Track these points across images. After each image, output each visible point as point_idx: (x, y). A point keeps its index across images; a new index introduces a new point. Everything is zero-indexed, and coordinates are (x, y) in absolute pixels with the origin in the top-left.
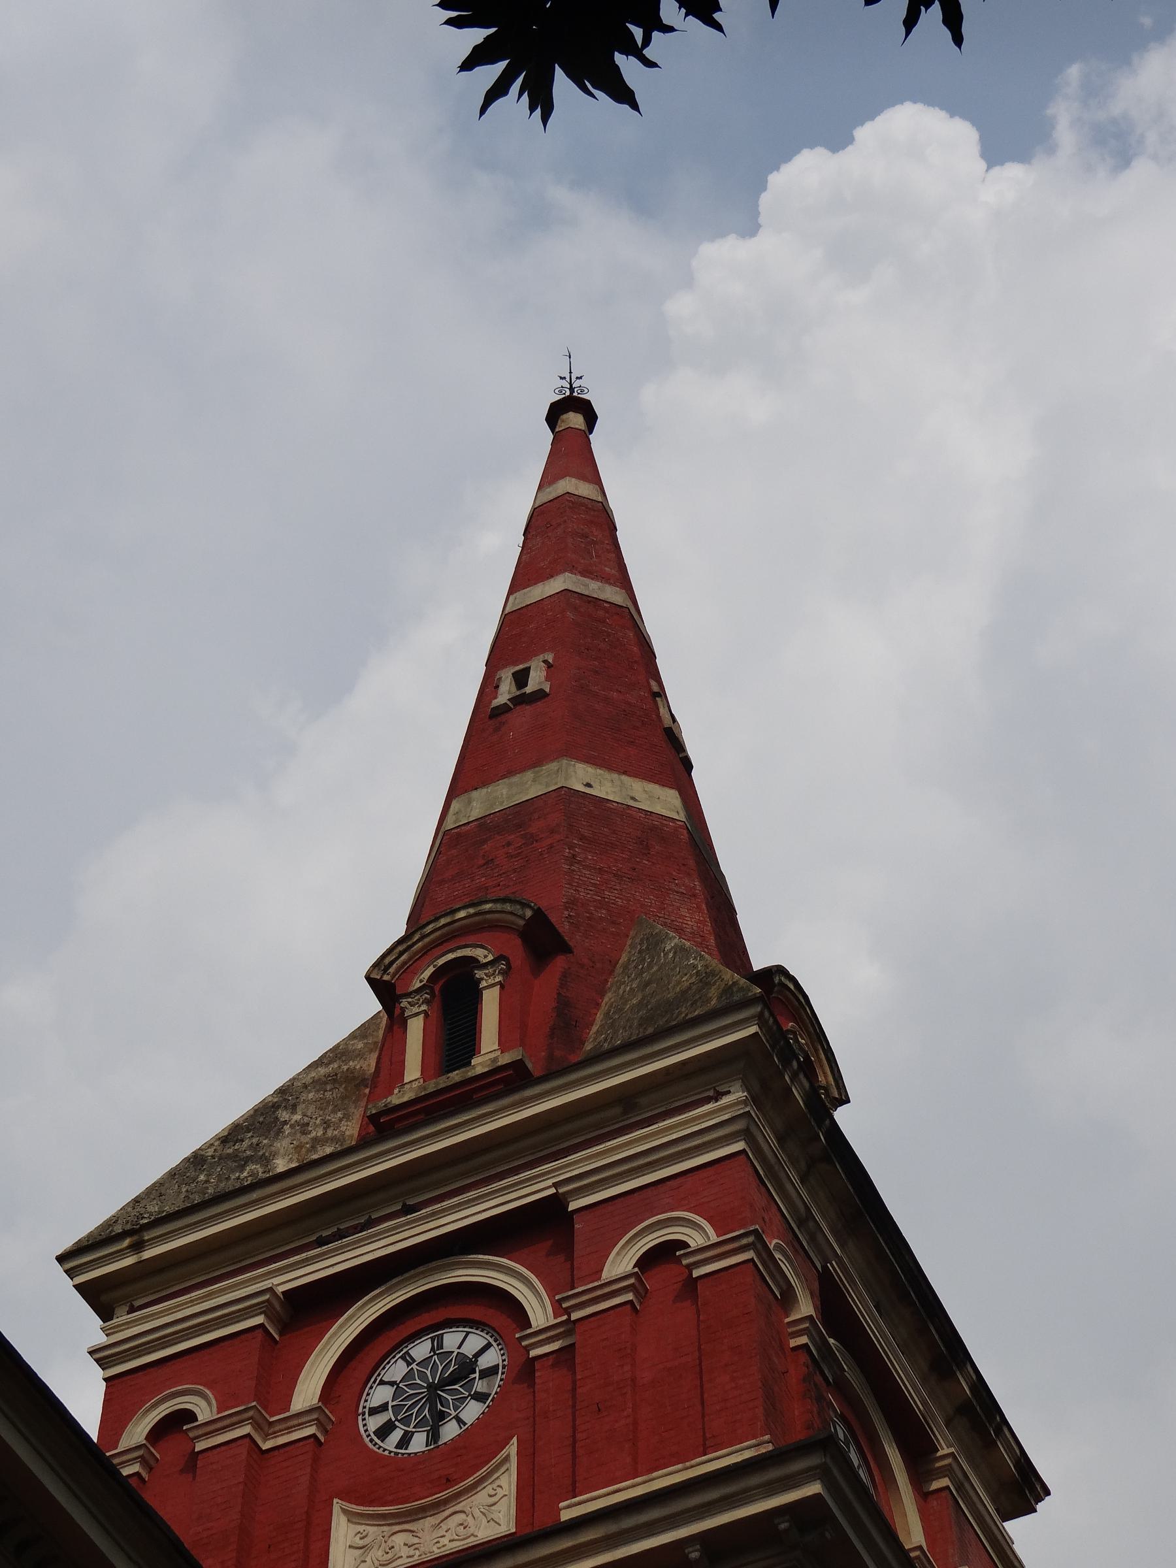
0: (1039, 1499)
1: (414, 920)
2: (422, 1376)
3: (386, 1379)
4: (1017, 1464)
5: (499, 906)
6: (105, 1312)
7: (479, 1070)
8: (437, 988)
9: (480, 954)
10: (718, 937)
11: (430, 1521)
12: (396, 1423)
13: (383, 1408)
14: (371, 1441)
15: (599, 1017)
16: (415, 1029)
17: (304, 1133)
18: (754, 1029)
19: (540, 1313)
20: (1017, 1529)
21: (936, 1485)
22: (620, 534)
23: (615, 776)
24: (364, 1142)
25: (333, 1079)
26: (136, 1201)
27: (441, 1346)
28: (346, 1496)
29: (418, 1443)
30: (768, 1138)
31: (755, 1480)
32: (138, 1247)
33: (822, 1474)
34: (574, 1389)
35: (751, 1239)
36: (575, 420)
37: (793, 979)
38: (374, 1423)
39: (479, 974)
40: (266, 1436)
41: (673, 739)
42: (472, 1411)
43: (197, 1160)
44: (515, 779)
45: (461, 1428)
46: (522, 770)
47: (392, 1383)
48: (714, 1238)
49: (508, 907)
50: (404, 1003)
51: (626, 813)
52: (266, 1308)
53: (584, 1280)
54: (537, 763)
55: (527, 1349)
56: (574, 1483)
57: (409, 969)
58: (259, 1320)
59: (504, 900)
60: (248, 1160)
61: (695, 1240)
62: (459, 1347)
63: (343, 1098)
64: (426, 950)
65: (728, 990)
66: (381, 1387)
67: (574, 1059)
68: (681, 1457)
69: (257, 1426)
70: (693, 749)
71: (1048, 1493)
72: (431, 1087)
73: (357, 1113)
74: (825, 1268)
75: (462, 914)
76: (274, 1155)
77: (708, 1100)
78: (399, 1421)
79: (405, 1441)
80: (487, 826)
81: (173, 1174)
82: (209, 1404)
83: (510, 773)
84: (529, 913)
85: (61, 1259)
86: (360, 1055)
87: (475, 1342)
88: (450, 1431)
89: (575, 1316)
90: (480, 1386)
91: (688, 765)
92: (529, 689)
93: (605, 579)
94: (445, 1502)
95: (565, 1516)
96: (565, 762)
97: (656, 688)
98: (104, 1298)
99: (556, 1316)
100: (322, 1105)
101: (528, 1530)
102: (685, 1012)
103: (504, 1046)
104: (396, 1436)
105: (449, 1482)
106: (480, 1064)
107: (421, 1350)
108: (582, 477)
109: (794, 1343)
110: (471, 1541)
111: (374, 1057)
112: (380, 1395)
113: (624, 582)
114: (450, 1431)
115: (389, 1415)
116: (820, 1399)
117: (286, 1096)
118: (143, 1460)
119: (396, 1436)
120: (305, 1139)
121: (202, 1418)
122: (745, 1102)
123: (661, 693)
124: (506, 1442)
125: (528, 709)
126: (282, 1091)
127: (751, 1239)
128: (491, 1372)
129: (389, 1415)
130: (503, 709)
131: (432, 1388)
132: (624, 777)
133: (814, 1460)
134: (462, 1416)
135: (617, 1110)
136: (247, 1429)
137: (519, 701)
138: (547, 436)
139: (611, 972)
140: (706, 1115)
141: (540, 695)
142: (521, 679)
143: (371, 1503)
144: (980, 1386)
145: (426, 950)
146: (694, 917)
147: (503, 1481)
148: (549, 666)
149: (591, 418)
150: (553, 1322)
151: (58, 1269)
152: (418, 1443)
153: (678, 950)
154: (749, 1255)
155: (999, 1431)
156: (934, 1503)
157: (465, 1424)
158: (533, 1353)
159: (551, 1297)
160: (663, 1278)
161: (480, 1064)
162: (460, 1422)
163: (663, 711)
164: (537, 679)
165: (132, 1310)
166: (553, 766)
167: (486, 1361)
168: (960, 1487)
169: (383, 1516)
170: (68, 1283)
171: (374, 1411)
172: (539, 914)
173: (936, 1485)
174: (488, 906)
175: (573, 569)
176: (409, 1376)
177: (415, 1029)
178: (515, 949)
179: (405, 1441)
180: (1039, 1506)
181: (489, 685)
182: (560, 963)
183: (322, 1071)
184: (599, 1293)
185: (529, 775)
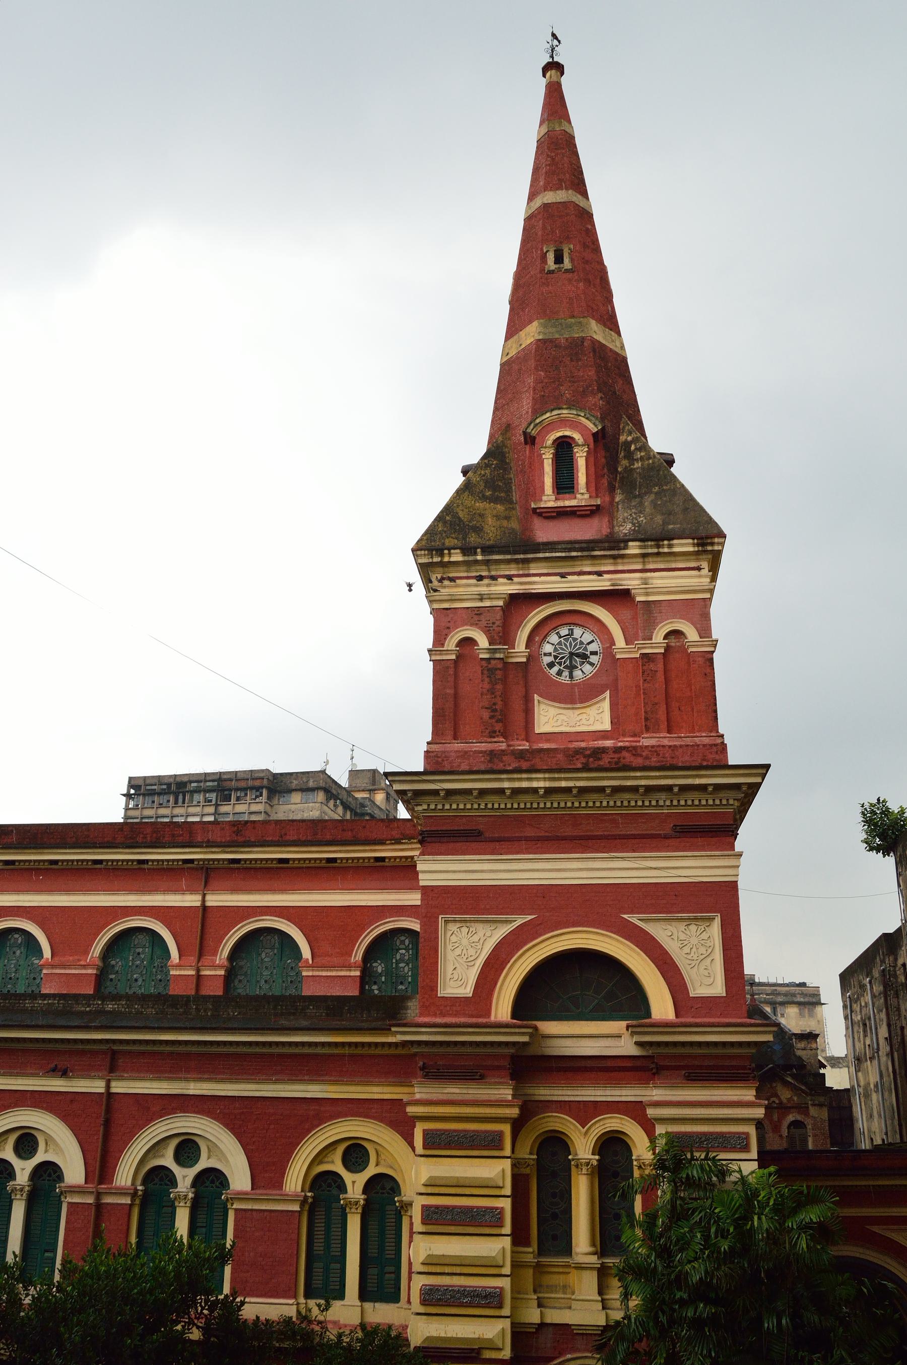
2: (566, 645)
13: (550, 654)
14: (546, 668)
19: (620, 641)
27: (572, 634)
38: (547, 660)
47: (553, 644)
87: (588, 637)
88: (577, 674)
107: (564, 631)
112: (548, 648)
119: (556, 669)
134: (583, 669)
167: (593, 647)
171: (545, 654)
176: (560, 643)
179: (559, 673)
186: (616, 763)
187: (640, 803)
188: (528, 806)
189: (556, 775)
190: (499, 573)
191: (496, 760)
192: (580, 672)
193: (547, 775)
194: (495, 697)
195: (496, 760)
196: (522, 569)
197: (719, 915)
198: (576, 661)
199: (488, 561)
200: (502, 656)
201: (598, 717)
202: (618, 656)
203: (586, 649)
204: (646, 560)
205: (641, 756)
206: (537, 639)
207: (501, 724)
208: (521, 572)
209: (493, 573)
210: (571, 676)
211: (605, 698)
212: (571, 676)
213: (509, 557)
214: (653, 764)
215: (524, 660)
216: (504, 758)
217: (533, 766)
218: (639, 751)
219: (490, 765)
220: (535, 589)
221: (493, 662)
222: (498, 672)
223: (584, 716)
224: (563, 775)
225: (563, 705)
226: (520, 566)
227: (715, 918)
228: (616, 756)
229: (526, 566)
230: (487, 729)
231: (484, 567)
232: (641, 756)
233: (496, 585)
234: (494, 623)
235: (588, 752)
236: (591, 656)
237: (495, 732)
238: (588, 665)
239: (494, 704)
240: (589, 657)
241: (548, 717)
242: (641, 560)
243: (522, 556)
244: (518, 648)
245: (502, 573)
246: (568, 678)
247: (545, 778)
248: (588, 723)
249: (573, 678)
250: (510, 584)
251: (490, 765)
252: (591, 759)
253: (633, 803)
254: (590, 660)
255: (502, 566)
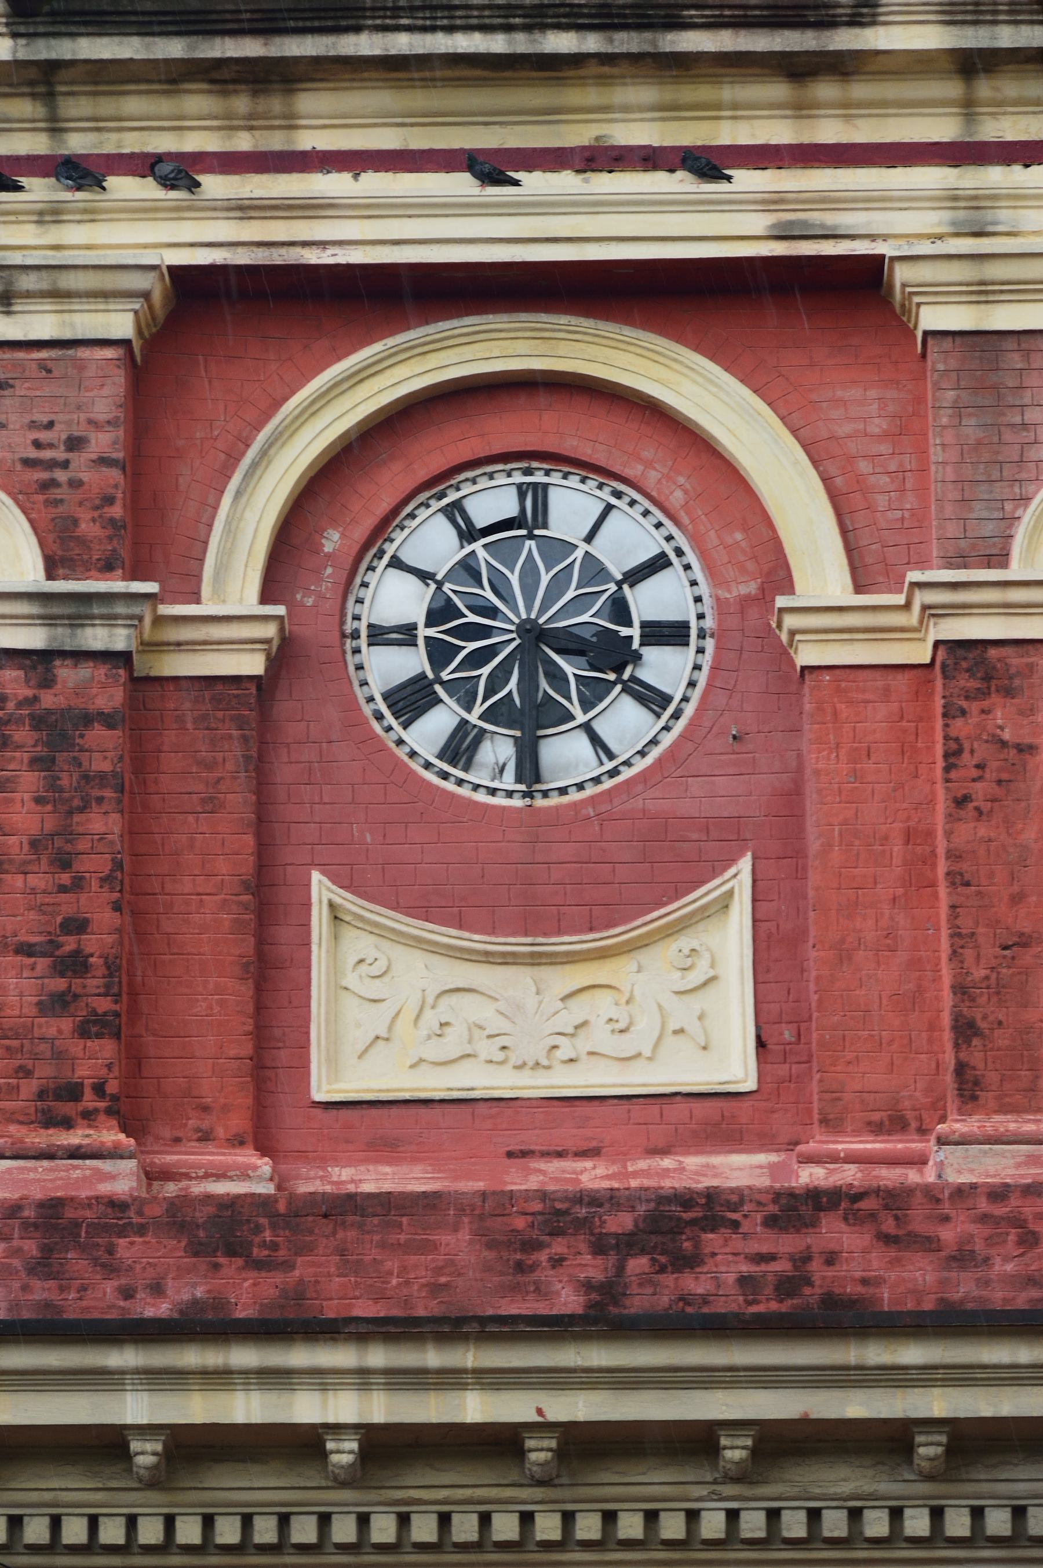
3: (408, 557)
12: (438, 688)
13: (406, 635)
14: (379, 717)
27: (541, 515)
45: (602, 764)
47: (424, 576)
62: (589, 538)
66: (395, 576)
78: (442, 683)
157: (611, 756)
171: (378, 635)
186: (787, 1287)
187: (917, 1524)
188: (265, 1531)
189: (433, 1357)
190: (112, 143)
191: (76, 1261)
192: (581, 744)
193: (377, 1357)
194: (78, 885)
195: (76, 1261)
196: (251, 123)
198: (557, 678)
199: (51, 68)
200: (119, 639)
201: (682, 1013)
202: (807, 655)
203: (620, 611)
204: (984, 88)
205: (929, 1244)
206: (332, 541)
207: (106, 1049)
208: (243, 142)
209: (78, 143)
211: (724, 903)
213: (173, 48)
214: (998, 1297)
215: (253, 664)
216: (126, 1249)
217: (298, 1294)
218: (919, 1221)
219: (42, 1291)
220: (323, 244)
221: (67, 674)
222: (98, 734)
223: (603, 1005)
224: (468, 1357)
225: (477, 941)
226: (241, 103)
228: (787, 1243)
229: (276, 104)
230: (28, 1073)
231: (25, 108)
232: (929, 1244)
233: (91, 215)
234: (74, 444)
235: (620, 1222)
236: (652, 654)
237: (73, 1092)
238: (627, 702)
239: (77, 926)
240: (636, 658)
241: (386, 1010)
242: (952, 88)
243: (250, 48)
244: (219, 595)
245: (132, 143)
246: (508, 781)
247: (363, 1372)
248: (626, 1045)
249: (538, 780)
250: (178, 212)
251: (42, 1291)
252: (638, 1264)
253: (877, 1524)
254: (644, 674)
255: (133, 105)
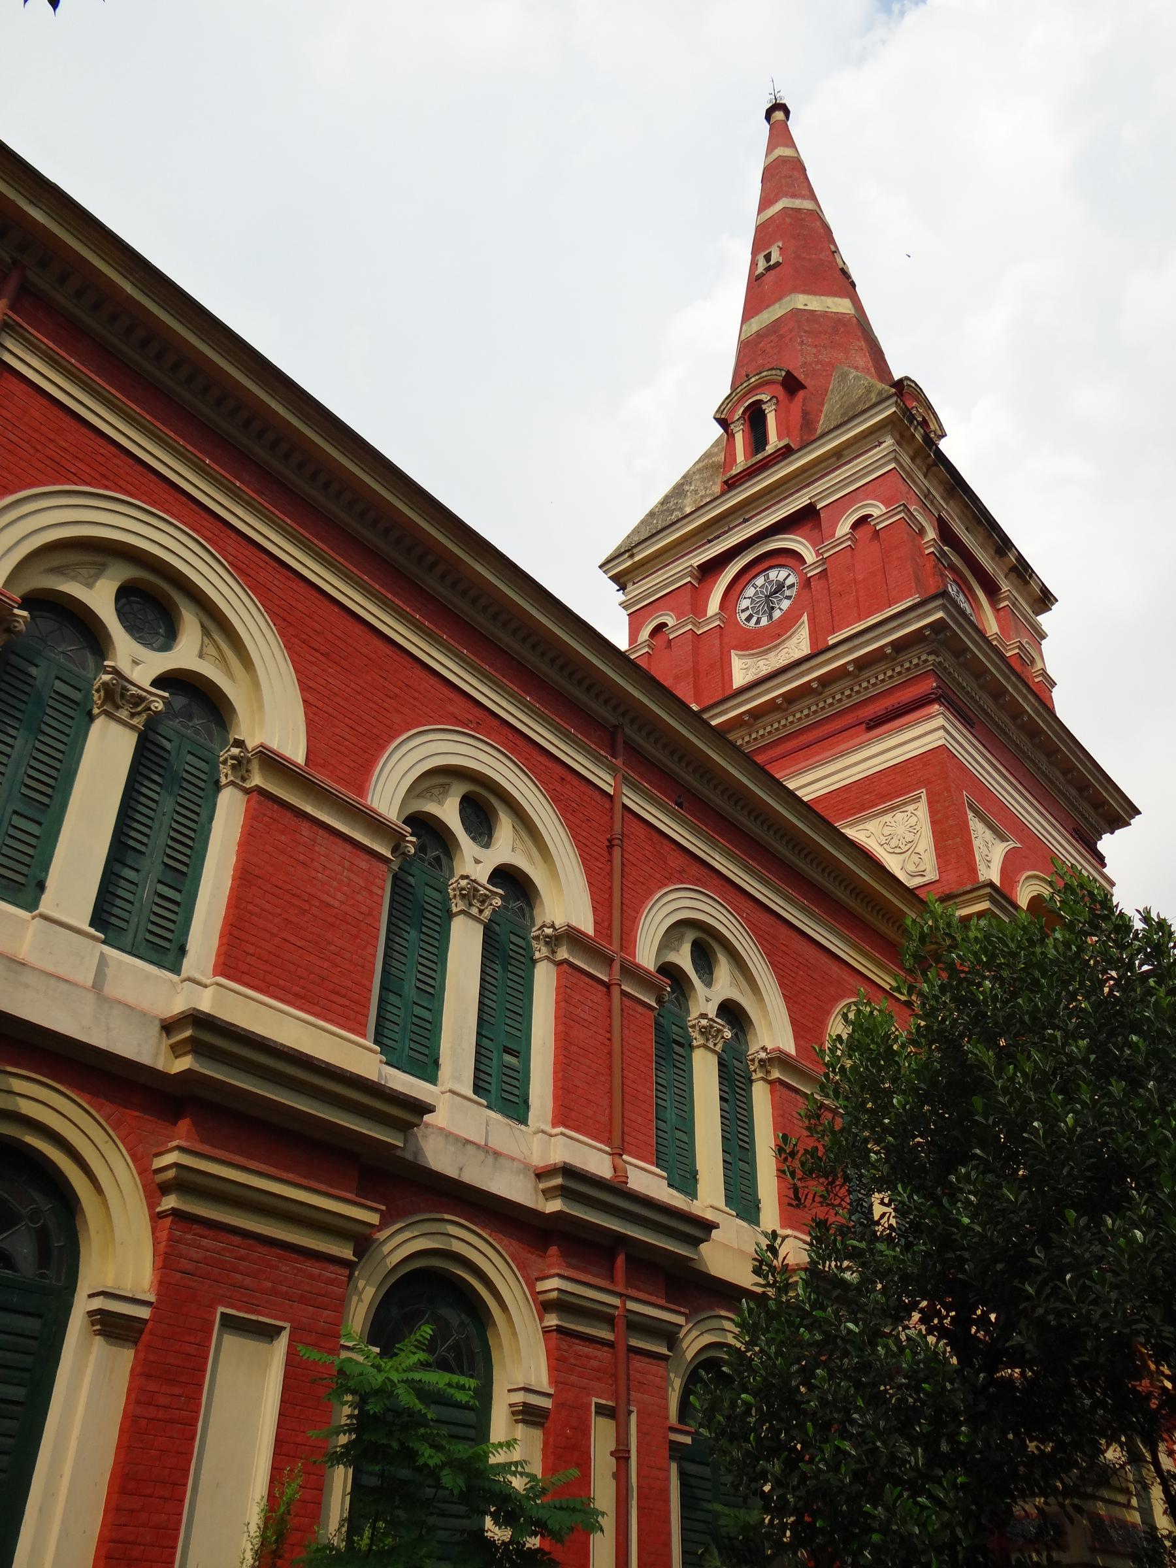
0: (1053, 604)
1: (734, 387)
4: (1041, 590)
5: (769, 373)
6: (623, 588)
7: (770, 452)
8: (746, 417)
9: (765, 397)
10: (876, 368)
11: (774, 653)
13: (747, 608)
15: (823, 416)
16: (739, 437)
17: (696, 494)
18: (894, 409)
19: (810, 556)
20: (1044, 620)
21: (1002, 605)
22: (808, 172)
23: (818, 297)
24: (723, 494)
25: (706, 467)
26: (628, 537)
28: (736, 648)
29: (764, 621)
30: (906, 460)
31: (913, 615)
32: (632, 556)
33: (943, 607)
34: (829, 588)
35: (902, 508)
36: (779, 115)
37: (913, 381)
38: (744, 616)
39: (764, 407)
40: (699, 629)
41: (845, 273)
42: (786, 604)
43: (652, 514)
44: (771, 309)
46: (774, 303)
47: (749, 598)
48: (885, 510)
49: (774, 372)
50: (732, 426)
51: (825, 315)
52: (691, 574)
53: (827, 539)
54: (780, 298)
55: (806, 573)
56: (833, 629)
57: (732, 411)
58: (689, 579)
59: (772, 369)
60: (673, 511)
61: (876, 512)
63: (711, 475)
64: (739, 400)
65: (880, 393)
67: (812, 438)
68: (880, 610)
69: (694, 625)
70: (855, 277)
71: (1057, 601)
72: (750, 463)
73: (719, 480)
74: (939, 515)
75: (753, 380)
76: (685, 506)
77: (876, 447)
79: (758, 622)
80: (761, 335)
81: (642, 522)
82: (671, 617)
83: (768, 306)
84: (784, 373)
85: (600, 567)
86: (717, 454)
87: (783, 573)
88: (777, 614)
89: (825, 556)
90: (788, 593)
91: (853, 285)
92: (772, 263)
93: (803, 197)
94: (779, 645)
95: (831, 643)
96: (793, 295)
97: (833, 249)
98: (622, 581)
99: (817, 557)
100: (703, 480)
101: (816, 651)
102: (861, 407)
103: (780, 438)
104: (754, 620)
105: (779, 636)
106: (770, 449)
107: (760, 581)
108: (786, 145)
109: (927, 552)
110: (792, 660)
111: (723, 453)
112: (745, 603)
113: (813, 197)
114: (777, 614)
115: (750, 611)
116: (942, 575)
117: (687, 479)
118: (649, 646)
119: (754, 620)
120: (697, 497)
121: (670, 625)
122: (893, 445)
123: (837, 251)
124: (802, 615)
125: (772, 272)
126: (684, 477)
127: (902, 508)
128: (792, 586)
129: (750, 611)
130: (762, 275)
131: (767, 597)
132: (822, 297)
133: (939, 602)
135: (834, 459)
136: (690, 627)
137: (768, 269)
138: (766, 126)
139: (826, 395)
140: (876, 454)
141: (778, 264)
142: (768, 258)
143: (747, 650)
144: (1020, 558)
145: (739, 400)
146: (863, 360)
147: (803, 632)
148: (781, 248)
149: (787, 113)
150: (816, 560)
151: (600, 572)
152: (764, 621)
153: (856, 378)
154: (902, 515)
155: (1031, 576)
156: (1002, 613)
158: (809, 575)
159: (814, 547)
160: (864, 531)
161: (770, 449)
162: (780, 609)
163: (839, 260)
164: (776, 257)
165: (634, 584)
166: (788, 298)
167: (788, 582)
168: (1014, 604)
169: (753, 654)
170: (605, 577)
171: (743, 611)
172: (788, 372)
173: (1002, 605)
174: (764, 374)
175: (786, 195)
176: (756, 593)
177: (739, 437)
178: (780, 391)
179: (758, 622)
180: (1053, 607)
181: (754, 264)
182: (801, 394)
183: (701, 465)
184: (835, 543)
185: (777, 305)
197: (924, 790)
210: (770, 617)
212: (770, 617)
227: (921, 797)
